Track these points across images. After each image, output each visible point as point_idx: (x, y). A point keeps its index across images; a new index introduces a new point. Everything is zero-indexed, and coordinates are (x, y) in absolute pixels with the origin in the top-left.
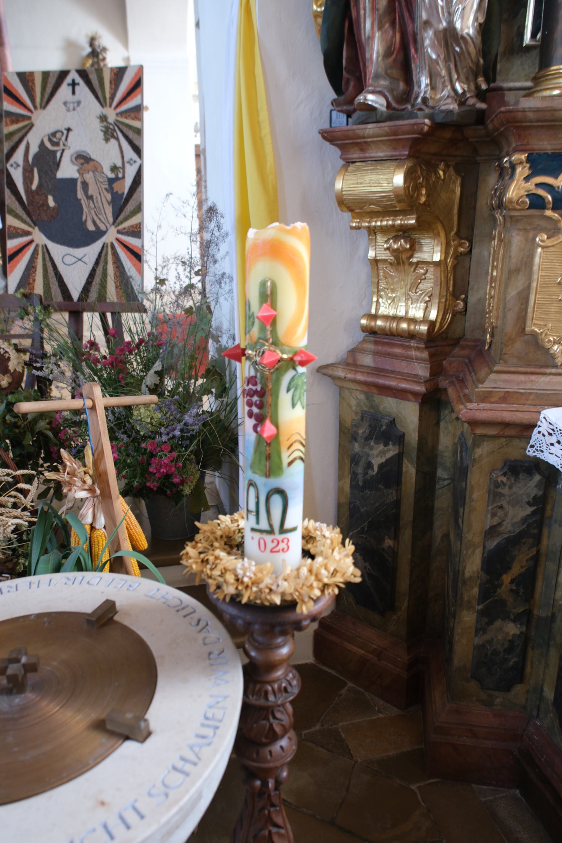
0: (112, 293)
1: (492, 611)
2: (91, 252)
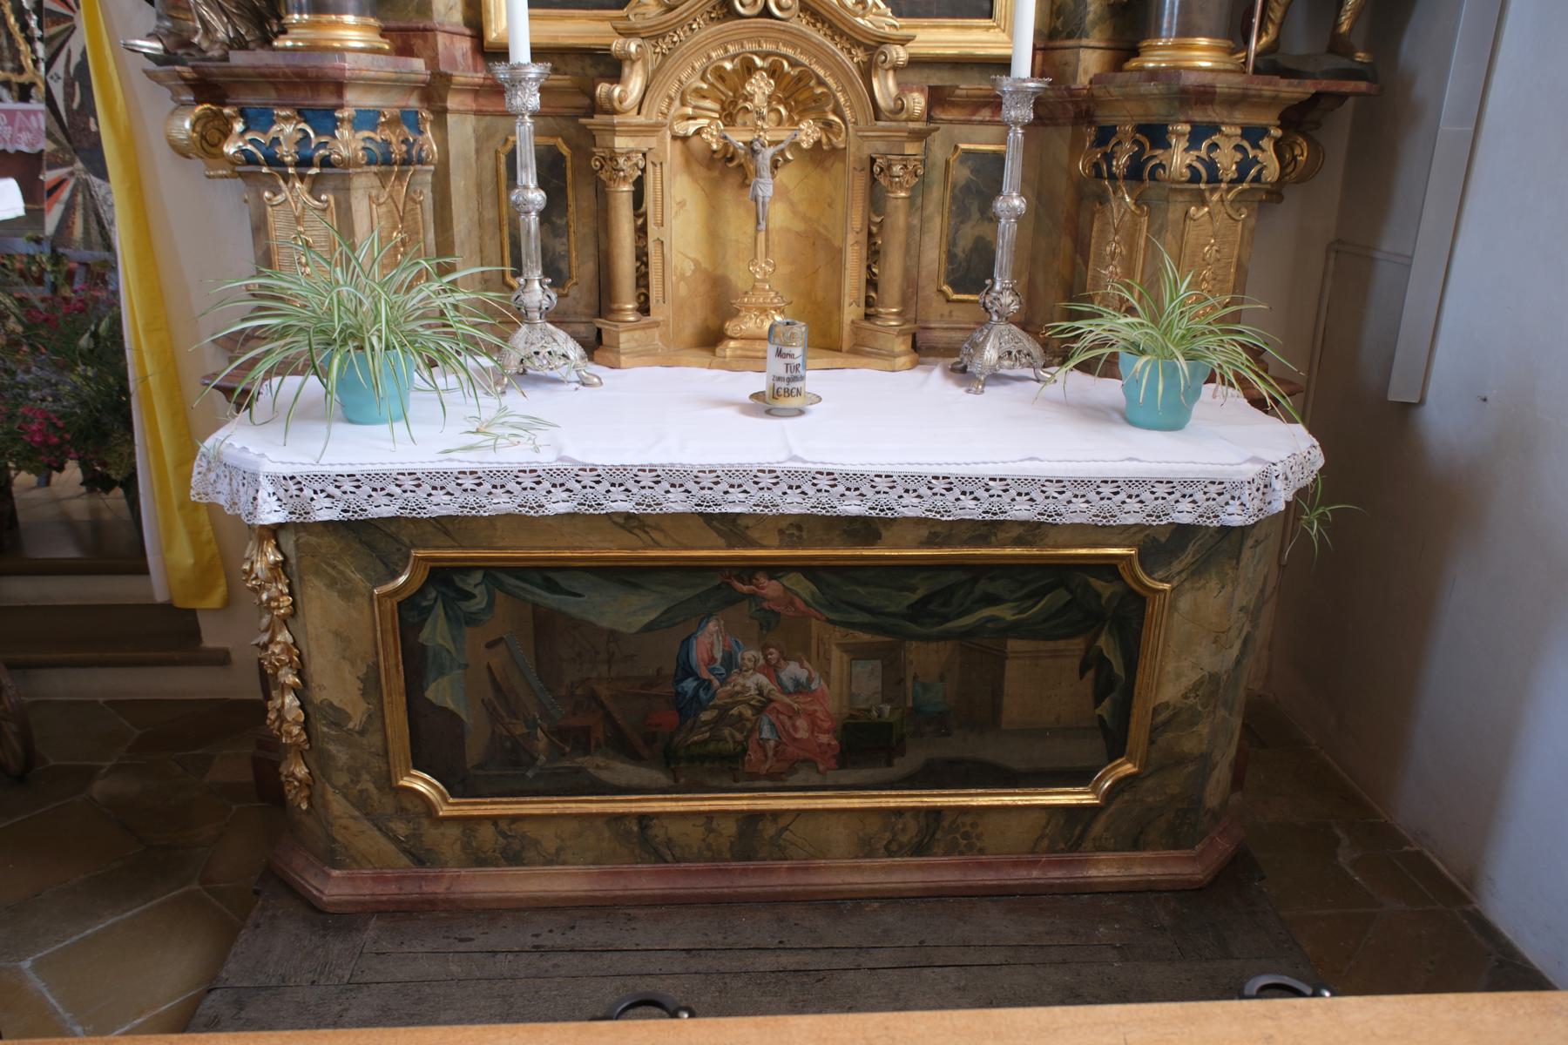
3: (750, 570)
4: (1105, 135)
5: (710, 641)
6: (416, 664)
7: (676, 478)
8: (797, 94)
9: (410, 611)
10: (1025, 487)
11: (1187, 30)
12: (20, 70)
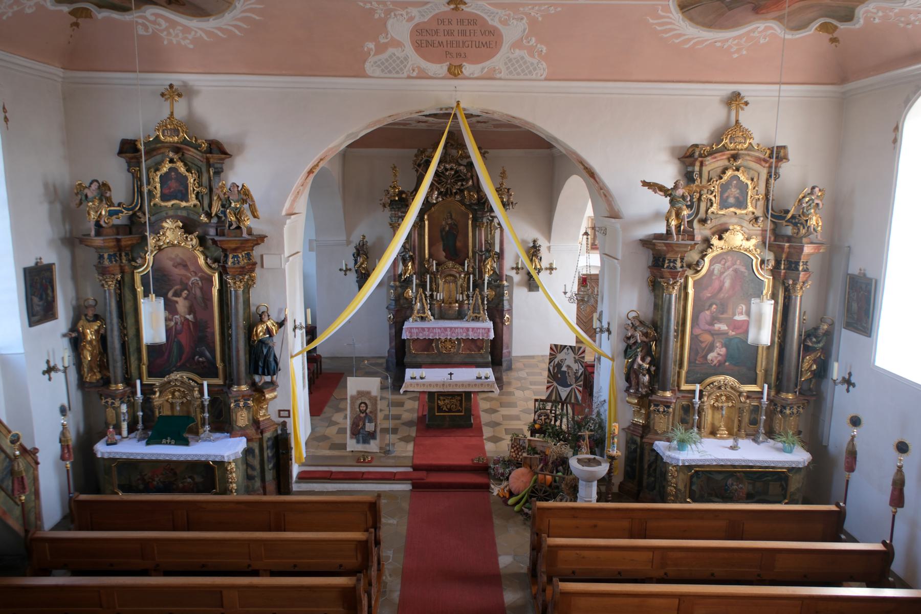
0: (573, 401)
1: (649, 475)
2: (568, 389)
3: (736, 472)
6: (691, 483)
8: (728, 398)
9: (692, 477)
10: (773, 462)
11: (788, 392)
12: (424, 313)
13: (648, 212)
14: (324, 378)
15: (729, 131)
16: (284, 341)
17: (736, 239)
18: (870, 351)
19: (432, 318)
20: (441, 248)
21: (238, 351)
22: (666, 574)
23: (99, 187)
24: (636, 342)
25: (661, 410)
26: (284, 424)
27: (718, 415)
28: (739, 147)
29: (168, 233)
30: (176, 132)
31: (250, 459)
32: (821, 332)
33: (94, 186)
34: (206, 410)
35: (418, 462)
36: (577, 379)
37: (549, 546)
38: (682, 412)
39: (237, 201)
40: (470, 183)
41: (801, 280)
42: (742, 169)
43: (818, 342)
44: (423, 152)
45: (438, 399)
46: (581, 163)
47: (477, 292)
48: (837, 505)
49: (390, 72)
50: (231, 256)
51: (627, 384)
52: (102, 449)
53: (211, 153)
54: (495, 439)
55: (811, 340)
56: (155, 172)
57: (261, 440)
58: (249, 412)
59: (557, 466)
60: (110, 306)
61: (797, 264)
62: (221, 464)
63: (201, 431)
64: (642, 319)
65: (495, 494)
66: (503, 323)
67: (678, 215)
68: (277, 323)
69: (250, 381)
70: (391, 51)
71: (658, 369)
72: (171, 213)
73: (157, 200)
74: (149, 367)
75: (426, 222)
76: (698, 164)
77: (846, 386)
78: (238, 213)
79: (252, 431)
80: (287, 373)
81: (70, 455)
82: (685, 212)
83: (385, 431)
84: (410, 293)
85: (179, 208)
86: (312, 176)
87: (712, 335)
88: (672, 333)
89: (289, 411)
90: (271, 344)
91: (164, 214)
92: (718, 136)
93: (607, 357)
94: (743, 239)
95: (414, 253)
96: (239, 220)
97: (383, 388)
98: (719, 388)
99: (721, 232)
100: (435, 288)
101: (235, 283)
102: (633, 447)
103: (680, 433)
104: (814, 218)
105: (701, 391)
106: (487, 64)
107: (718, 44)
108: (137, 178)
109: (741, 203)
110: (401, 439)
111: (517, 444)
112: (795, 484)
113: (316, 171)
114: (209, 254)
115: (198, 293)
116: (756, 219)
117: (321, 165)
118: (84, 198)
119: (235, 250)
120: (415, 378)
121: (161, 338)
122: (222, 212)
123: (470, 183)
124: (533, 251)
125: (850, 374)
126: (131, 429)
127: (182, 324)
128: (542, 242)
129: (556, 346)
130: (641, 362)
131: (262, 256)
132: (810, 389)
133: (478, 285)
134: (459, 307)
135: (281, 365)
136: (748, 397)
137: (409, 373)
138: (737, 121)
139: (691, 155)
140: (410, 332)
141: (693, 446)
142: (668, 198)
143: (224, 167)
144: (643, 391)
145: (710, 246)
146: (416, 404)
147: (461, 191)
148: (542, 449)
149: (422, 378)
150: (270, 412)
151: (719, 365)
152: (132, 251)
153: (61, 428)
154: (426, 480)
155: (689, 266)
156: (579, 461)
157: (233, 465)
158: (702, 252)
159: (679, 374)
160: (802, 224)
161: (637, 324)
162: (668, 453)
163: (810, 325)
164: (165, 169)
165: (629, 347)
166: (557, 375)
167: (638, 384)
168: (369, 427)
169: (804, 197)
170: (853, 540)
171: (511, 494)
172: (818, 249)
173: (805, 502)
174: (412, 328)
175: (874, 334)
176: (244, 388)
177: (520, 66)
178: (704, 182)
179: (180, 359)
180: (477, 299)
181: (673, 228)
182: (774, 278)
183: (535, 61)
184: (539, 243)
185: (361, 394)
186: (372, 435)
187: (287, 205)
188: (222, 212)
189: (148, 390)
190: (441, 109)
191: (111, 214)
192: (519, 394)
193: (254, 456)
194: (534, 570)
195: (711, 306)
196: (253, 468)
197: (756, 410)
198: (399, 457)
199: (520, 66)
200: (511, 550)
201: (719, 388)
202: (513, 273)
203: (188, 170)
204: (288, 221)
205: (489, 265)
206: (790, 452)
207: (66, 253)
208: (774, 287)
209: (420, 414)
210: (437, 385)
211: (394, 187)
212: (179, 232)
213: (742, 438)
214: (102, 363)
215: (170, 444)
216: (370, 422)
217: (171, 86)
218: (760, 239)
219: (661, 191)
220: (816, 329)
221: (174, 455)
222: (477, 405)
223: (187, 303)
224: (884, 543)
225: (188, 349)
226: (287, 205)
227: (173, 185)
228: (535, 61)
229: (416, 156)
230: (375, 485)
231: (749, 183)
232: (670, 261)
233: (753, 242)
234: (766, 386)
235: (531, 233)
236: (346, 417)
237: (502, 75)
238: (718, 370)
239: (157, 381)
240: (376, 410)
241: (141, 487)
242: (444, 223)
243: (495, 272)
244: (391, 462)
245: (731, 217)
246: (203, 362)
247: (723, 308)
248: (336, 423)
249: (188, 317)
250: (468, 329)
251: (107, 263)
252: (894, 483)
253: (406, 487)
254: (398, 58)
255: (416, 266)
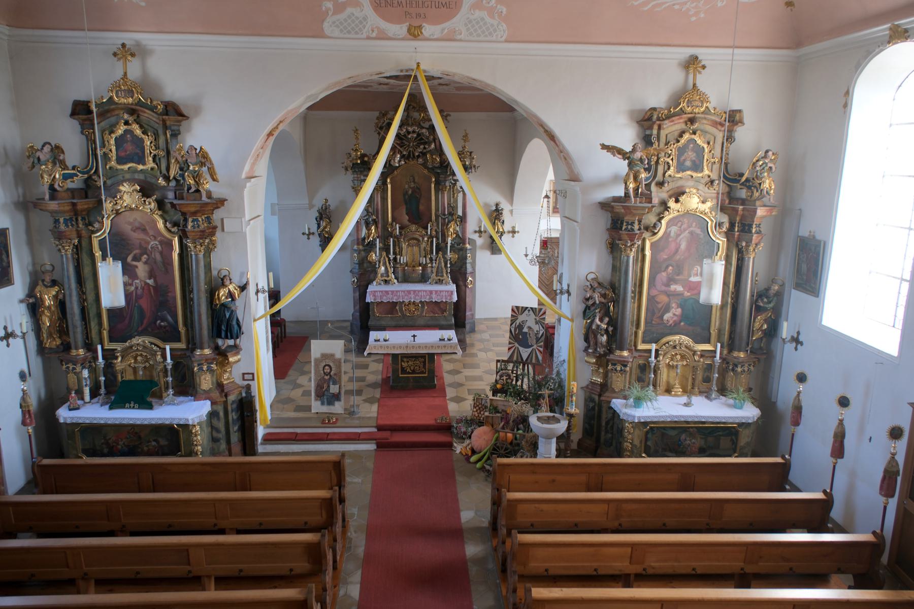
1: (607, 432)
2: (530, 350)
3: (689, 428)
4: (728, 363)
5: (683, 437)
6: (647, 439)
7: (683, 417)
8: (683, 357)
9: (647, 433)
10: (724, 418)
11: (740, 351)
13: (607, 175)
14: (288, 342)
15: (687, 94)
16: (246, 305)
17: (692, 202)
18: (818, 310)
19: (395, 281)
20: (404, 211)
21: (200, 316)
22: (620, 525)
23: (52, 150)
24: (594, 303)
25: (619, 369)
26: (248, 387)
27: (673, 374)
28: (696, 110)
29: (126, 197)
30: (130, 93)
31: (215, 422)
32: (772, 292)
33: (47, 149)
34: (169, 374)
35: (381, 422)
36: (538, 340)
37: (509, 501)
38: (638, 371)
39: (196, 164)
40: (433, 146)
41: (753, 242)
42: (698, 132)
43: (769, 302)
44: (384, 115)
45: (402, 361)
46: (542, 126)
47: (440, 255)
48: (783, 457)
49: (349, 32)
50: (190, 220)
51: (586, 345)
52: (64, 414)
53: (167, 114)
54: (458, 400)
55: (762, 300)
56: (110, 134)
57: (226, 403)
58: (213, 376)
59: (518, 424)
60: (68, 271)
61: (750, 226)
62: (186, 427)
63: (164, 395)
64: (600, 280)
65: (458, 452)
66: (466, 286)
67: (636, 178)
68: (239, 287)
69: (212, 345)
70: (349, 10)
71: (615, 329)
72: (127, 176)
73: (113, 163)
74: (110, 332)
75: (389, 186)
76: (656, 127)
77: (794, 344)
78: (197, 176)
79: (216, 395)
80: (250, 337)
81: (31, 421)
82: (643, 175)
83: (349, 393)
84: (374, 257)
85: (135, 171)
86: (272, 139)
87: (668, 296)
88: (629, 294)
89: (253, 374)
90: (233, 308)
91: (120, 177)
92: (676, 99)
93: (567, 318)
94: (699, 202)
95: (377, 217)
96: (197, 183)
97: (347, 351)
98: (675, 347)
99: (678, 195)
100: (398, 252)
101: (195, 247)
102: (591, 405)
103: (636, 390)
104: (767, 181)
105: (657, 351)
106: (446, 25)
107: (677, 7)
108: (91, 140)
109: (697, 167)
110: (365, 401)
111: (479, 403)
112: (745, 438)
113: (276, 134)
114: (168, 218)
115: (158, 257)
116: (712, 182)
117: (281, 127)
118: (36, 161)
119: (194, 213)
120: (379, 340)
121: (121, 302)
122: (180, 175)
123: (433, 146)
124: (496, 215)
125: (798, 333)
126: (94, 394)
127: (143, 288)
128: (505, 206)
129: (517, 307)
130: (599, 323)
131: (222, 220)
132: (761, 348)
133: (441, 249)
134: (423, 270)
135: (244, 329)
136: (702, 356)
137: (373, 335)
138: (694, 85)
139: (650, 119)
140: (374, 296)
141: (649, 403)
142: (627, 161)
143: (182, 129)
144: (601, 350)
145: (667, 208)
146: (380, 367)
147: (424, 154)
148: (503, 408)
149: (385, 340)
150: (233, 375)
151: (675, 325)
152: (88, 214)
153: (21, 394)
154: (389, 439)
155: (647, 228)
156: (539, 419)
157: (198, 428)
158: (659, 214)
159: (636, 333)
160: (755, 187)
161: (596, 285)
162: (625, 410)
163: (762, 286)
164: (121, 130)
165: (587, 308)
166: (519, 336)
167: (596, 344)
168: (334, 389)
169: (758, 161)
170: (796, 489)
171: (474, 452)
172: (771, 211)
173: (754, 455)
174: (376, 291)
175: (821, 295)
176: (207, 351)
177: (480, 27)
178: (662, 145)
179: (142, 324)
180: (440, 263)
181: (631, 191)
182: (728, 240)
183: (495, 23)
184: (501, 206)
185: (325, 356)
186: (337, 397)
187: (247, 168)
188: (180, 175)
189: (109, 355)
190: (402, 71)
191: (65, 177)
192: (481, 355)
193: (219, 419)
194: (494, 525)
195: (667, 267)
196: (218, 431)
197: (710, 368)
198: (363, 418)
199: (480, 27)
200: (473, 505)
201: (675, 347)
202: (475, 237)
203: (144, 133)
204: (248, 185)
205: (452, 228)
206: (741, 408)
207: (21, 218)
208: (728, 249)
209: (384, 376)
210: (400, 347)
211: (356, 150)
212: (137, 196)
213: (696, 395)
214: (62, 330)
215: (134, 408)
216: (334, 383)
217: (123, 45)
218: (715, 201)
219: (619, 154)
220: (767, 290)
221: (138, 419)
222: (440, 366)
223: (146, 268)
224: (825, 492)
225: (151, 313)
226: (247, 168)
227: (129, 147)
228: (495, 23)
229: (378, 118)
230: (339, 446)
231: (705, 146)
232: (628, 224)
233: (709, 204)
234: (719, 345)
235: (493, 197)
236: (310, 380)
237: (462, 37)
238: (674, 329)
239: (118, 346)
240: (340, 372)
241: (106, 451)
242: (407, 186)
243: (457, 235)
244: (356, 422)
245: (688, 179)
246: (165, 327)
247: (679, 269)
248: (300, 386)
249: (148, 281)
250: (431, 292)
251: (62, 227)
252: (836, 435)
253: (371, 446)
254: (357, 18)
255: (380, 230)
